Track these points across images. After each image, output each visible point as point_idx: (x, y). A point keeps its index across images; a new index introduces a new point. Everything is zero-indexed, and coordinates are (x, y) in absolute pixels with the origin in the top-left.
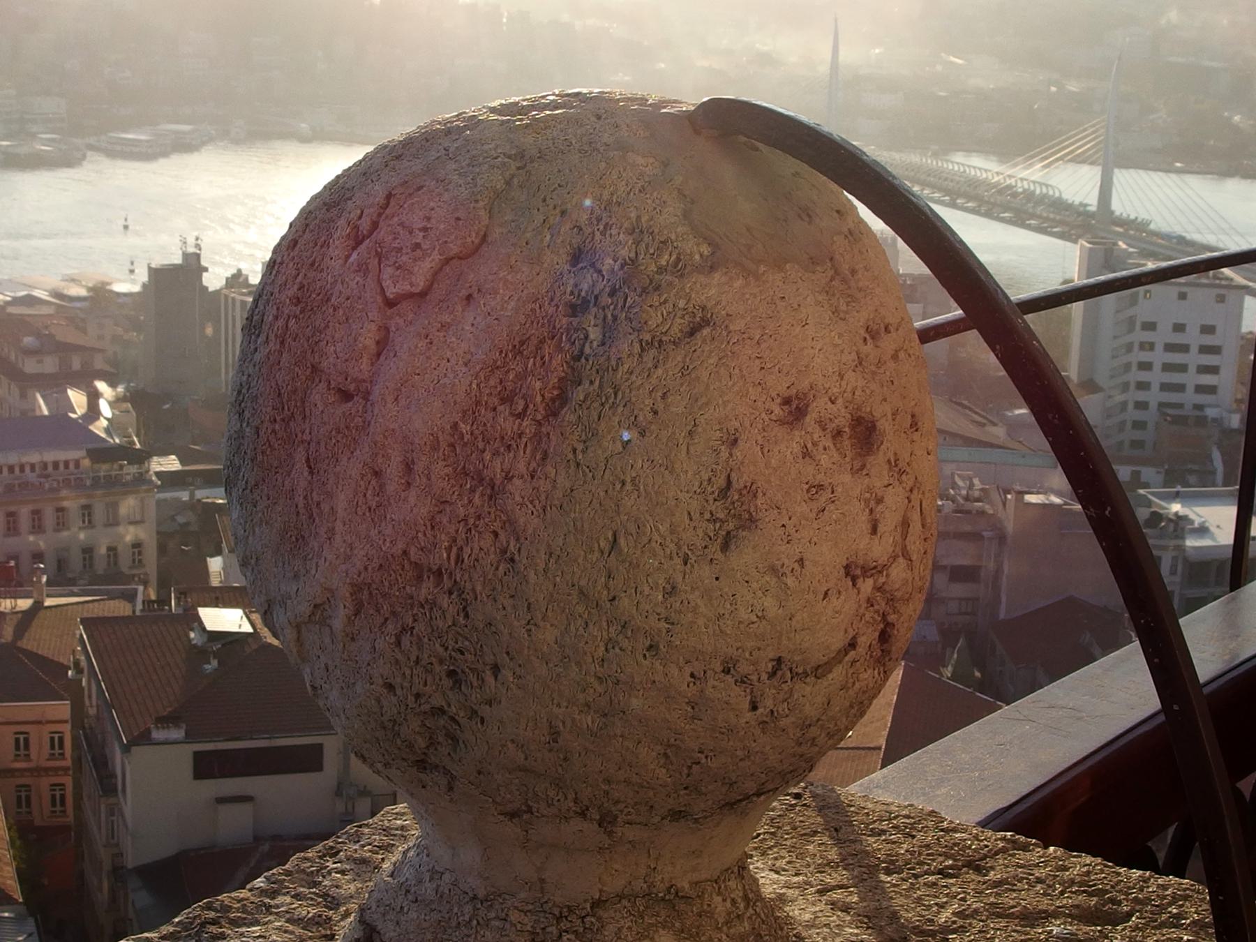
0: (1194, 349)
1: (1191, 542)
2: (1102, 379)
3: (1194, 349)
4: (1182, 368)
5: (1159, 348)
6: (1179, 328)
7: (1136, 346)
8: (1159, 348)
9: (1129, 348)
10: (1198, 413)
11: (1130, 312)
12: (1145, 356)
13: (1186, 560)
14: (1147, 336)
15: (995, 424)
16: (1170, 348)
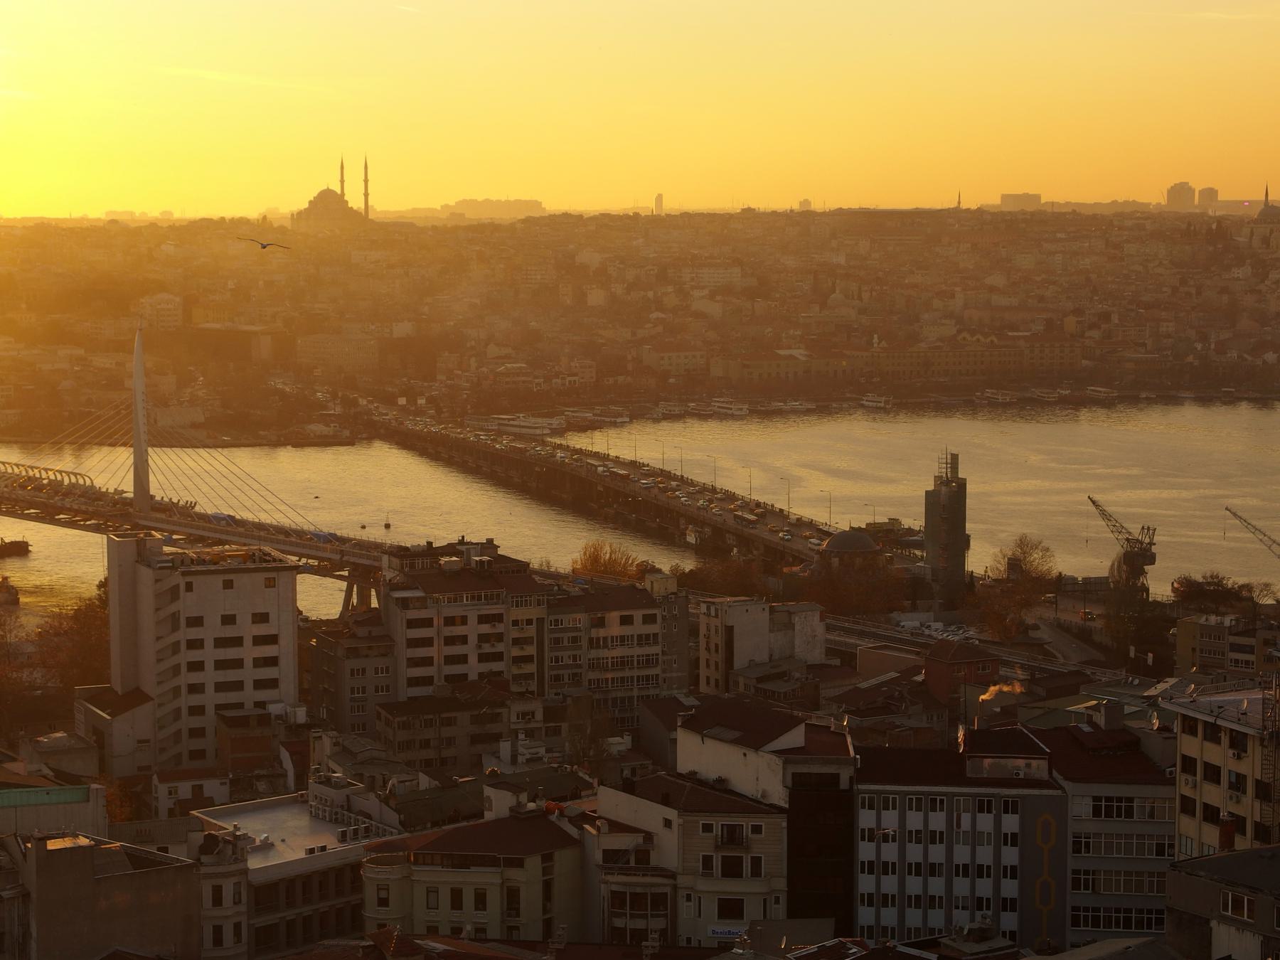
0: (248, 642)
1: (254, 863)
2: (149, 687)
3: (248, 642)
4: (238, 664)
5: (209, 644)
6: (229, 620)
7: (183, 646)
8: (209, 644)
9: (175, 648)
10: (260, 711)
11: (173, 608)
12: (195, 655)
13: (250, 885)
14: (194, 633)
15: (14, 760)
16: (221, 643)
